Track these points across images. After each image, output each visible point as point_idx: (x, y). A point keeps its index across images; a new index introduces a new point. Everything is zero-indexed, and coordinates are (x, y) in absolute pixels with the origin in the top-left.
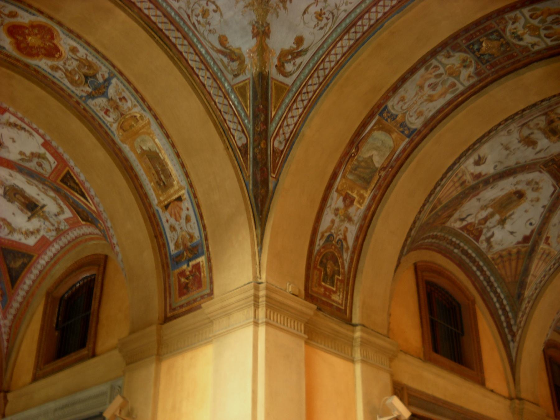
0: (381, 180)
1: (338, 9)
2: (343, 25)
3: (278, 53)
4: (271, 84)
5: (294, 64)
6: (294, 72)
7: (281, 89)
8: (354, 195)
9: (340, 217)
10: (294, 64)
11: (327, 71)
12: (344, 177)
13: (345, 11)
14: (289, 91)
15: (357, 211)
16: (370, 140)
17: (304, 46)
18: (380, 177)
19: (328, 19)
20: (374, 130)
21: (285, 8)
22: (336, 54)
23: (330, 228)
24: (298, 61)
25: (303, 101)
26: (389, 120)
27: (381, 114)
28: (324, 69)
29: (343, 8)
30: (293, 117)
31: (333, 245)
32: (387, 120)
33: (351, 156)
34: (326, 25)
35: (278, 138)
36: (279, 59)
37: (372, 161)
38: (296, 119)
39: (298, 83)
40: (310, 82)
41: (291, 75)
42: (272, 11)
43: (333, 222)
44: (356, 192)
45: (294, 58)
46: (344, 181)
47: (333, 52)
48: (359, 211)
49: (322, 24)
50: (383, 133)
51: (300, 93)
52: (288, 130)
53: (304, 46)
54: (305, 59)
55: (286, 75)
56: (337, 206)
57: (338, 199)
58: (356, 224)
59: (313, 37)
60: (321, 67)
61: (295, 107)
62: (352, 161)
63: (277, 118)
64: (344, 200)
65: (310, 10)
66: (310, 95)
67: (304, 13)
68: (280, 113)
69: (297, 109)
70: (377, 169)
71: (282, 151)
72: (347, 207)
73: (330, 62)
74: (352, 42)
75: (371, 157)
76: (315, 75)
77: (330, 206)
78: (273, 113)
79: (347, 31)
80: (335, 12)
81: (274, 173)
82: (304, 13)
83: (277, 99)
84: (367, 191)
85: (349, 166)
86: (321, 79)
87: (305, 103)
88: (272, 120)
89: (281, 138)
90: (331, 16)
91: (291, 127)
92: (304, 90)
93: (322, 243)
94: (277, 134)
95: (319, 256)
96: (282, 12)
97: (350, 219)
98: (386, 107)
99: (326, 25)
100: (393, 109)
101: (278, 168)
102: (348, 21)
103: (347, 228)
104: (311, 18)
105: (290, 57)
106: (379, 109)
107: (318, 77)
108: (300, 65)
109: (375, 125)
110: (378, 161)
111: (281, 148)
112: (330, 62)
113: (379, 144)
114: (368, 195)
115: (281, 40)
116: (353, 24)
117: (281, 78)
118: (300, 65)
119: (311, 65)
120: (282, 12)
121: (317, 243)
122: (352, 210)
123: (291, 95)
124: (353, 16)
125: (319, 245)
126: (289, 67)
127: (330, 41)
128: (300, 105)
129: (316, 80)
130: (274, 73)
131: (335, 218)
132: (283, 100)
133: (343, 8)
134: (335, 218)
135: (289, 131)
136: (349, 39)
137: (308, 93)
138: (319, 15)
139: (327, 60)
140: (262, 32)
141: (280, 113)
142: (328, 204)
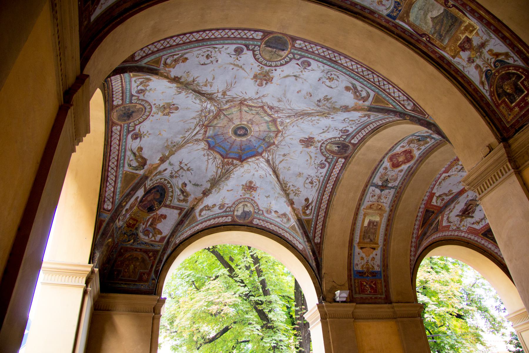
0: (457, 5)
1: (324, 70)
2: (332, 65)
3: (356, 101)
4: (375, 105)
5: (361, 91)
6: (366, 91)
7: (377, 99)
8: (463, 37)
9: (477, 58)
10: (361, 91)
11: (364, 69)
12: (444, 49)
13: (323, 67)
14: (378, 94)
15: (479, 33)
16: (417, 23)
17: (350, 85)
18: (454, 6)
19: (331, 75)
20: (409, 21)
21: (331, 98)
22: (352, 65)
23: (481, 71)
24: (359, 89)
25: (384, 85)
26: (400, 8)
27: (394, 18)
28: (363, 71)
29: (323, 68)
30: (394, 93)
31: (495, 73)
32: (400, 11)
33: (429, 41)
34: (335, 75)
35: (406, 106)
36: (360, 100)
37: (436, 17)
38: (396, 91)
39: (373, 88)
40: (372, 80)
41: (368, 92)
42: (333, 105)
43: (477, 67)
44: (461, 35)
45: (358, 92)
46: (448, 49)
47: (351, 67)
48: (480, 33)
49: (335, 77)
50: (411, 10)
51: (379, 87)
52: (402, 98)
53: (350, 85)
54: (357, 84)
55: (368, 95)
56: (466, 59)
57: (461, 58)
58: (490, 37)
59: (344, 81)
60: (361, 73)
61: (388, 90)
62: (433, 39)
63: (394, 104)
64: (464, 49)
65: (329, 85)
66: (380, 79)
67: (331, 88)
68: (391, 101)
69: (389, 89)
70: (445, 10)
71: (414, 104)
72: (471, 48)
73: (357, 68)
74: (342, 57)
75: (433, 19)
76: (367, 77)
77: (464, 67)
78: (391, 106)
79: (336, 62)
80: (326, 72)
81: (425, 115)
82: (331, 88)
83: (383, 102)
84: (464, 22)
85: (437, 43)
86: (370, 72)
87: (385, 83)
88: (395, 108)
89: (406, 103)
90: (329, 73)
91: (400, 94)
92: (377, 83)
93: (487, 87)
94: (404, 106)
95: (494, 95)
96: (333, 100)
97: (483, 45)
98: (388, 15)
99: (335, 75)
100: (389, 7)
101: (423, 112)
102: (329, 63)
103: (490, 50)
104: (333, 84)
105: (358, 94)
106: (390, 21)
107: (368, 75)
108: (362, 87)
109: (404, 21)
110: (438, 10)
111: (412, 104)
112: (357, 68)
113: (422, 12)
114: (469, 20)
115: (349, 99)
116: (330, 60)
117: (371, 99)
118: (362, 87)
119: (361, 80)
120: (333, 100)
121: (484, 91)
122: (476, 42)
123: (381, 93)
124: (325, 61)
125: (487, 90)
126: (364, 94)
127: (344, 71)
128: (387, 87)
129: (371, 76)
130: (367, 103)
131: (475, 64)
132: (383, 98)
133: (323, 68)
134: (475, 64)
135: (402, 96)
136: (340, 60)
137: (379, 81)
138: (331, 79)
139: (356, 70)
140: (346, 109)
141: (391, 101)
142: (462, 69)
